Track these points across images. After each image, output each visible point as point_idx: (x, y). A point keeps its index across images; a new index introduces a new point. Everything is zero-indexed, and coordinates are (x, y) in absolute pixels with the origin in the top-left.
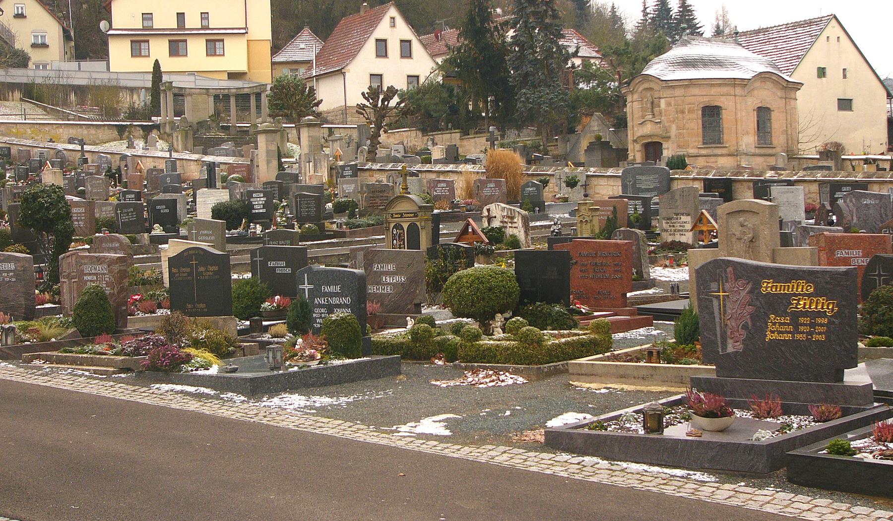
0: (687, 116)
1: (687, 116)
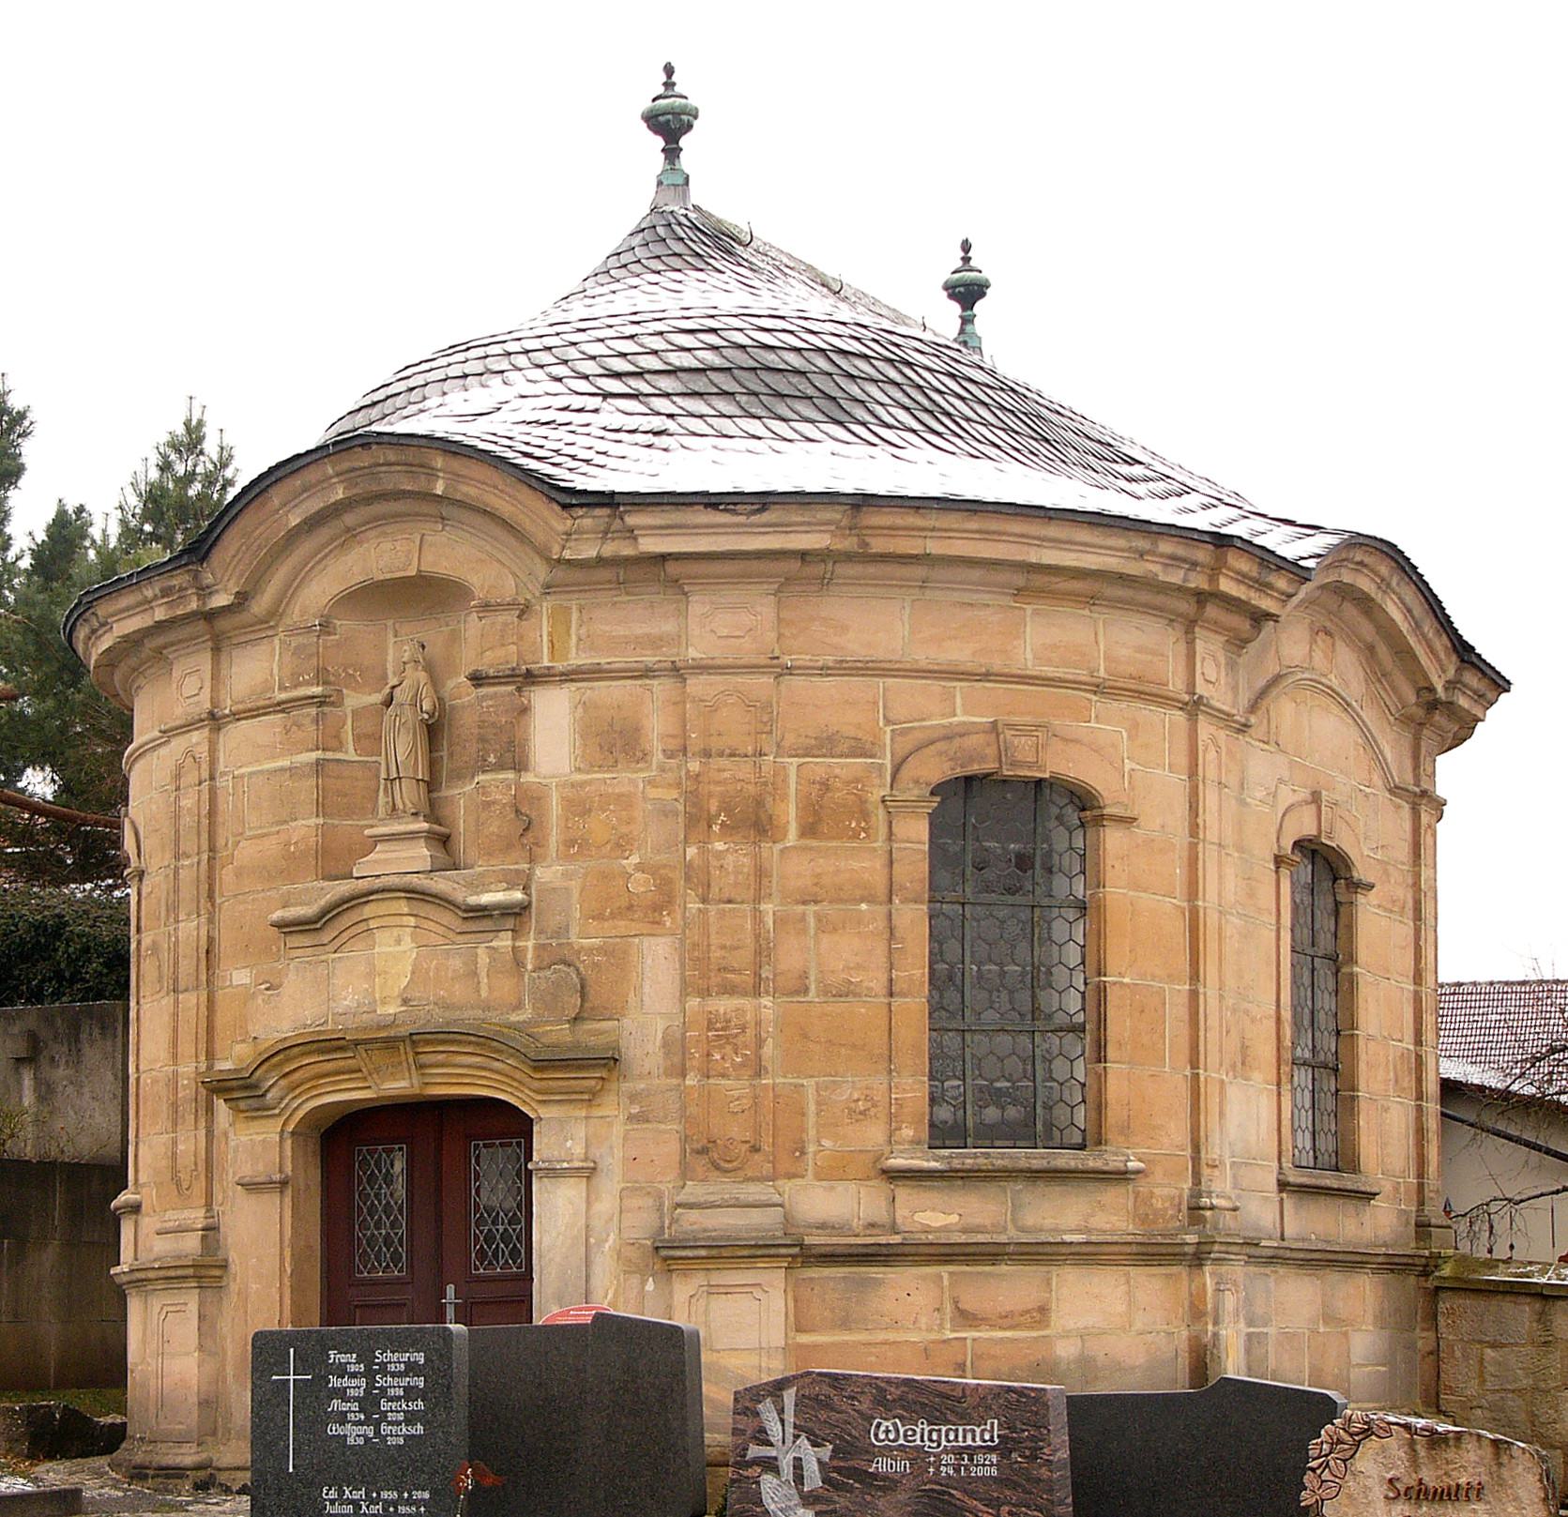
0: (793, 860)
1: (793, 860)
